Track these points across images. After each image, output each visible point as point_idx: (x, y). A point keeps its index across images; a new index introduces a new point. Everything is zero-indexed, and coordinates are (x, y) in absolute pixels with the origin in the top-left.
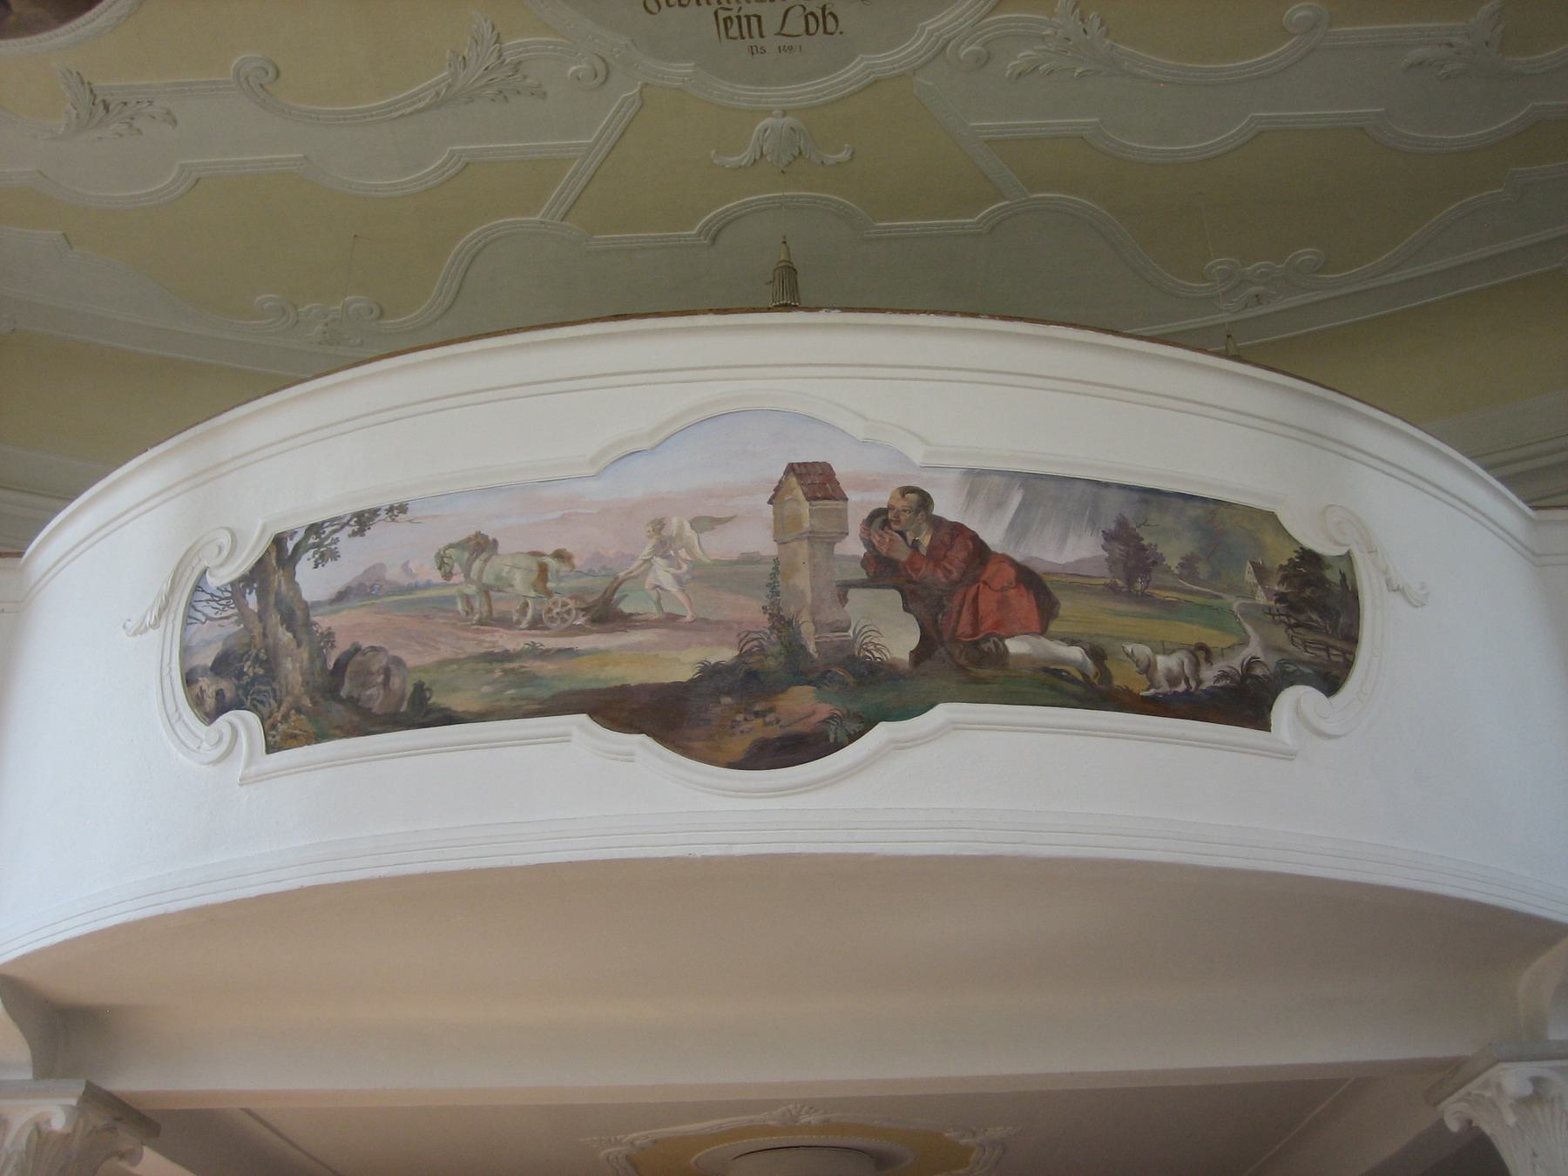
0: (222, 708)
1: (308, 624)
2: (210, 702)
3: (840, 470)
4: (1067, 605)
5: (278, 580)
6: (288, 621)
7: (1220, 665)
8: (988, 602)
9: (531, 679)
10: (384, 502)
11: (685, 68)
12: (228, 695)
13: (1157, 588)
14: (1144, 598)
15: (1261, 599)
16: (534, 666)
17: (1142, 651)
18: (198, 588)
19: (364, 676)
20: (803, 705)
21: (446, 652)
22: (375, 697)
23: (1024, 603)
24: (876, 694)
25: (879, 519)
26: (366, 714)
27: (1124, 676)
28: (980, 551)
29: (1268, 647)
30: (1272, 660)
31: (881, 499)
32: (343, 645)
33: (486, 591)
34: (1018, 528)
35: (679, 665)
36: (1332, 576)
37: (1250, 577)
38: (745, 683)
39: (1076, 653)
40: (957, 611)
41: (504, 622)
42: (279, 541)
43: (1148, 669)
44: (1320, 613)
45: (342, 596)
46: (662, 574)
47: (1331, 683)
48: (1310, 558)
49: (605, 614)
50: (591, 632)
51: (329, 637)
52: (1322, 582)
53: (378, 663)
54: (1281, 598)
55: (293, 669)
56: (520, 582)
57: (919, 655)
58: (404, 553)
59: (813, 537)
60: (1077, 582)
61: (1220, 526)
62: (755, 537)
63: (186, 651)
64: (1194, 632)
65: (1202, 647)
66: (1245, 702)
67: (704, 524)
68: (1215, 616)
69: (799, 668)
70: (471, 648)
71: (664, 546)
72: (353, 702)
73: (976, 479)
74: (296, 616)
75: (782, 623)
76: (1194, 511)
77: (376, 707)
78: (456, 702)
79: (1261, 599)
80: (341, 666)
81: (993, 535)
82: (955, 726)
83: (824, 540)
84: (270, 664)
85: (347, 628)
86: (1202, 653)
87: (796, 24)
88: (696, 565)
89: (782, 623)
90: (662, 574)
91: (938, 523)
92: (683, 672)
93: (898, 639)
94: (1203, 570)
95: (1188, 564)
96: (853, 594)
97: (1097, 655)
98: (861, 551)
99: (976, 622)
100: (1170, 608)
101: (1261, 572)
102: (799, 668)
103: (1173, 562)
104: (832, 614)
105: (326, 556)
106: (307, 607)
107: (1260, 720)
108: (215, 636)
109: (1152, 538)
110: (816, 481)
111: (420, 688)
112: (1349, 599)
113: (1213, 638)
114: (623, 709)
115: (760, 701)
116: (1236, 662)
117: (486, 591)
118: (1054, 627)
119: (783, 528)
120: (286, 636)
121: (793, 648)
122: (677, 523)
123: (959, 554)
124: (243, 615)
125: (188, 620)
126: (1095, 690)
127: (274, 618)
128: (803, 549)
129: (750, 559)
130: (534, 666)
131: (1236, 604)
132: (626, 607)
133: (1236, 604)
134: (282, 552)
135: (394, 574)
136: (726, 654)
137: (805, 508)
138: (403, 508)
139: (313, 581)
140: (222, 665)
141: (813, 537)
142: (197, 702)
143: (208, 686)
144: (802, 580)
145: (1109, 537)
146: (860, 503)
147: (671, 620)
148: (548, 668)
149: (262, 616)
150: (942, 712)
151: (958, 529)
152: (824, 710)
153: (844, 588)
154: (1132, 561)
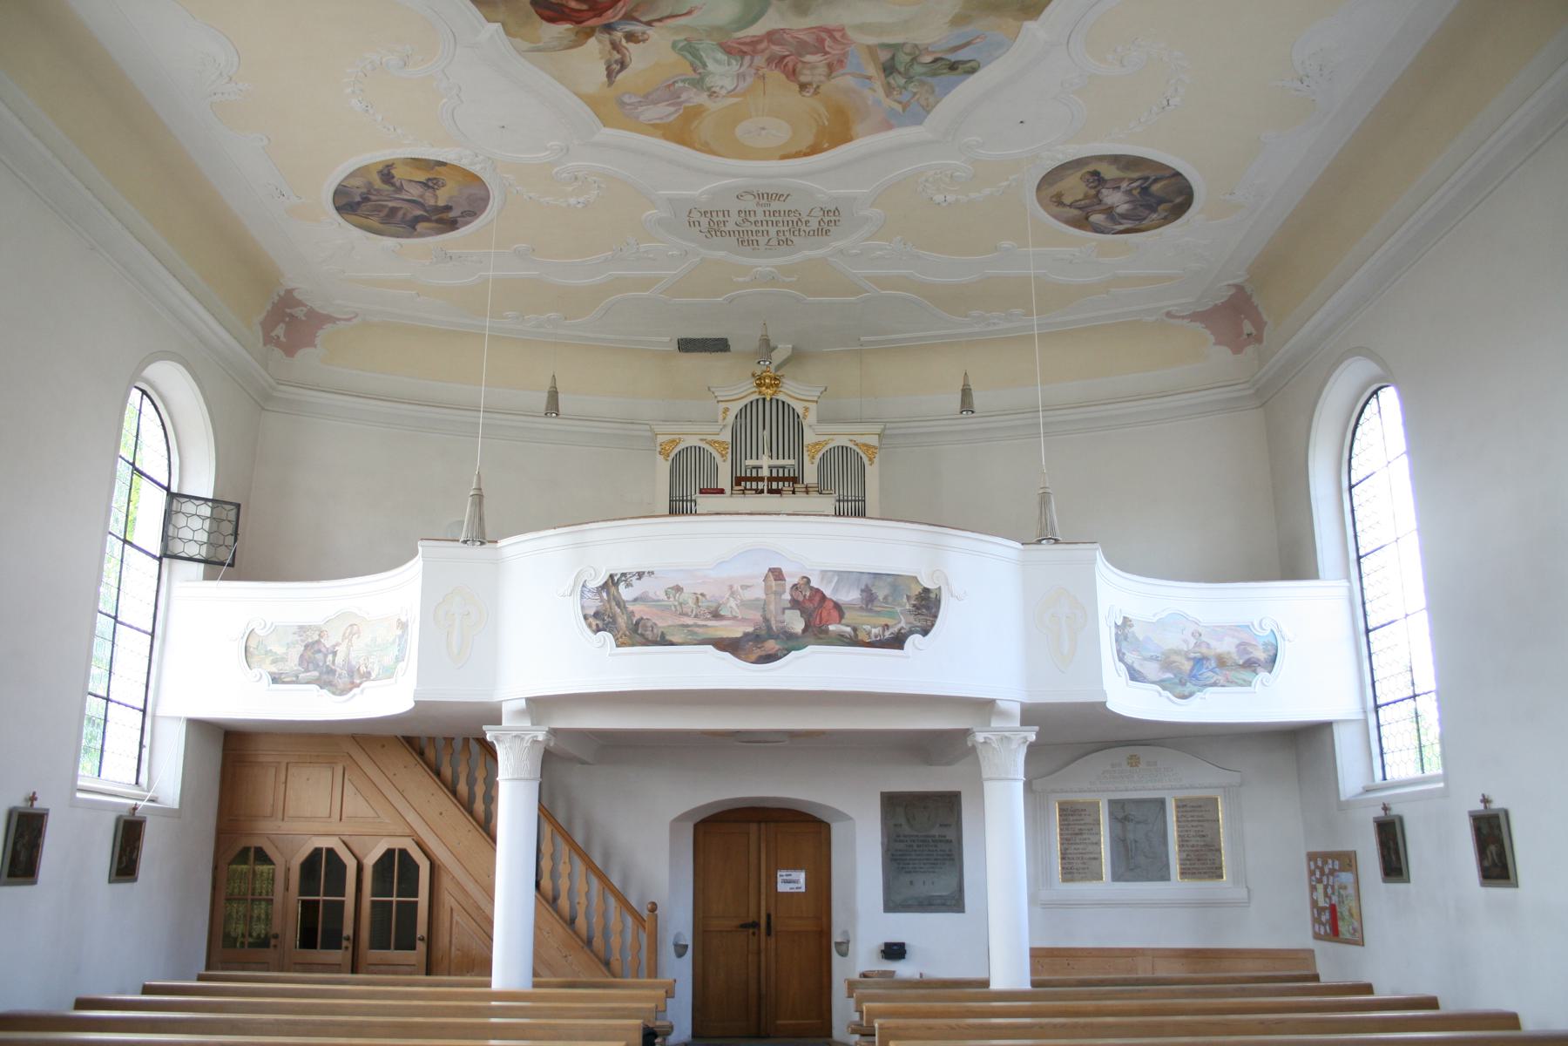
0: (598, 630)
4: (847, 615)
5: (613, 590)
6: (618, 604)
8: (825, 614)
11: (722, 253)
14: (871, 610)
19: (645, 627)
20: (772, 645)
22: (649, 634)
23: (835, 614)
24: (791, 642)
25: (795, 587)
27: (862, 636)
28: (823, 597)
30: (907, 627)
31: (796, 581)
32: (637, 617)
34: (836, 590)
35: (737, 632)
36: (933, 596)
38: (756, 638)
40: (816, 616)
41: (686, 615)
43: (869, 633)
44: (927, 606)
45: (635, 600)
47: (925, 632)
48: (926, 590)
49: (716, 615)
55: (622, 621)
56: (691, 603)
57: (804, 631)
58: (654, 588)
59: (776, 593)
60: (851, 607)
61: (896, 582)
62: (758, 593)
66: (897, 642)
67: (744, 587)
68: (892, 615)
69: (771, 635)
71: (733, 594)
74: (620, 603)
75: (766, 620)
76: (890, 579)
78: (674, 639)
80: (637, 623)
81: (828, 593)
83: (779, 594)
84: (614, 622)
85: (639, 610)
86: (887, 626)
87: (774, 242)
89: (766, 620)
90: (732, 603)
92: (739, 635)
93: (797, 624)
95: (886, 598)
97: (855, 630)
101: (908, 598)
102: (771, 635)
104: (780, 618)
105: (628, 585)
107: (901, 647)
108: (594, 605)
109: (874, 589)
110: (777, 574)
112: (938, 602)
113: (890, 622)
115: (758, 645)
119: (767, 589)
121: (769, 628)
122: (737, 587)
123: (817, 598)
124: (602, 600)
126: (854, 641)
131: (898, 609)
133: (898, 609)
134: (612, 582)
135: (651, 595)
136: (750, 629)
139: (625, 593)
140: (596, 615)
141: (776, 593)
142: (590, 626)
143: (594, 622)
144: (772, 607)
146: (790, 581)
147: (735, 618)
148: (700, 630)
150: (810, 648)
151: (818, 591)
154: (869, 597)
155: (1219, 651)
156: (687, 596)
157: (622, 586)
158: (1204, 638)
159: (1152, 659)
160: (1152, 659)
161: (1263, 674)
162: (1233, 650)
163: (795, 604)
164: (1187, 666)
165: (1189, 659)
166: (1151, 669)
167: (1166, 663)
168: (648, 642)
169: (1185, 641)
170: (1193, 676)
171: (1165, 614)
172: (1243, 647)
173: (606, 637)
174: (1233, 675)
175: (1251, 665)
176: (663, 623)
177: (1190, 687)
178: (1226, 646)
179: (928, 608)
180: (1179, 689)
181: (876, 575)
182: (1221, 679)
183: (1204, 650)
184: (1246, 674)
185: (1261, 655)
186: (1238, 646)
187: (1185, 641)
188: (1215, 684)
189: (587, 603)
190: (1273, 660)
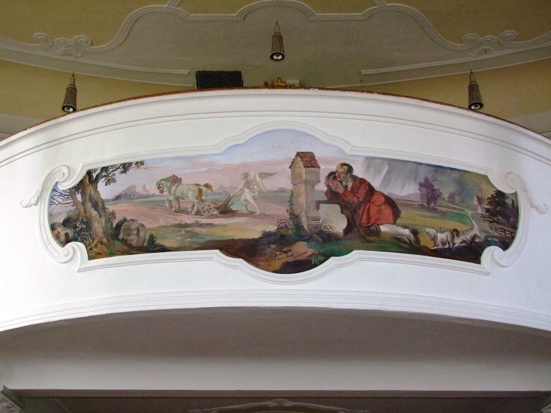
0: (68, 240)
1: (104, 208)
2: (63, 238)
3: (317, 155)
4: (404, 213)
5: (90, 189)
6: (95, 206)
7: (462, 238)
8: (373, 211)
9: (197, 235)
10: (134, 160)
12: (71, 235)
13: (439, 206)
14: (434, 210)
15: (480, 211)
16: (198, 230)
17: (432, 231)
18: (54, 190)
19: (129, 231)
20: (302, 249)
21: (162, 223)
22: (134, 240)
23: (387, 211)
24: (329, 246)
25: (332, 175)
26: (130, 246)
27: (425, 241)
28: (371, 190)
29: (481, 231)
30: (482, 236)
31: (333, 168)
32: (119, 218)
33: (177, 199)
34: (386, 181)
35: (254, 232)
36: (509, 201)
37: (476, 202)
39: (407, 232)
40: (362, 214)
41: (185, 212)
42: (89, 173)
43: (434, 239)
44: (504, 215)
46: (248, 195)
47: (505, 245)
48: (500, 195)
49: (225, 211)
50: (220, 217)
51: (113, 214)
52: (504, 204)
53: (134, 226)
54: (488, 211)
55: (99, 226)
56: (192, 196)
57: (347, 231)
58: (142, 182)
59: (306, 182)
60: (408, 204)
61: (465, 181)
63: (50, 216)
64: (452, 224)
65: (455, 230)
66: (471, 253)
67: (264, 175)
68: (461, 218)
70: (172, 222)
71: (248, 184)
72: (124, 241)
73: (370, 161)
74: (98, 205)
75: (294, 216)
76: (455, 175)
77: (134, 244)
78: (167, 243)
79: (480, 211)
80: (119, 226)
81: (376, 184)
82: (361, 259)
83: (311, 184)
84: (88, 224)
85: (121, 211)
86: (455, 232)
88: (261, 192)
89: (294, 216)
90: (248, 195)
91: (355, 178)
92: (256, 235)
93: (338, 223)
94: (457, 199)
95: (452, 196)
96: (322, 206)
97: (415, 232)
98: (325, 189)
99: (369, 219)
100: (444, 214)
101: (480, 200)
102: (301, 235)
103: (446, 196)
104: (313, 213)
106: (103, 201)
107: (477, 260)
108: (64, 210)
109: (437, 185)
110: (308, 160)
111: (152, 237)
112: (515, 211)
113: (460, 227)
114: (234, 248)
115: (284, 248)
116: (468, 237)
117: (177, 199)
118: (399, 221)
119: (295, 178)
120: (94, 213)
121: (299, 227)
123: (362, 191)
124: (75, 203)
125: (51, 203)
126: (414, 247)
127: (89, 205)
128: (302, 188)
129: (283, 191)
130: (198, 230)
131: (469, 213)
132: (233, 208)
133: (469, 213)
134: (90, 179)
135: (139, 190)
136: (272, 228)
137: (303, 170)
138: (142, 163)
139: (105, 191)
140: (67, 223)
141: (306, 182)
142: (57, 237)
144: (302, 200)
145: (421, 185)
146: (325, 169)
147: (251, 214)
148: (203, 231)
149: (83, 204)
150: (355, 254)
151: (363, 181)
152: (310, 251)
153: (319, 203)
154: (430, 193)
156: (187, 189)
157: (101, 185)
163: (333, 197)
168: (131, 249)
173: (78, 248)
176: (151, 223)
179: (505, 216)
181: (438, 168)
189: (57, 209)
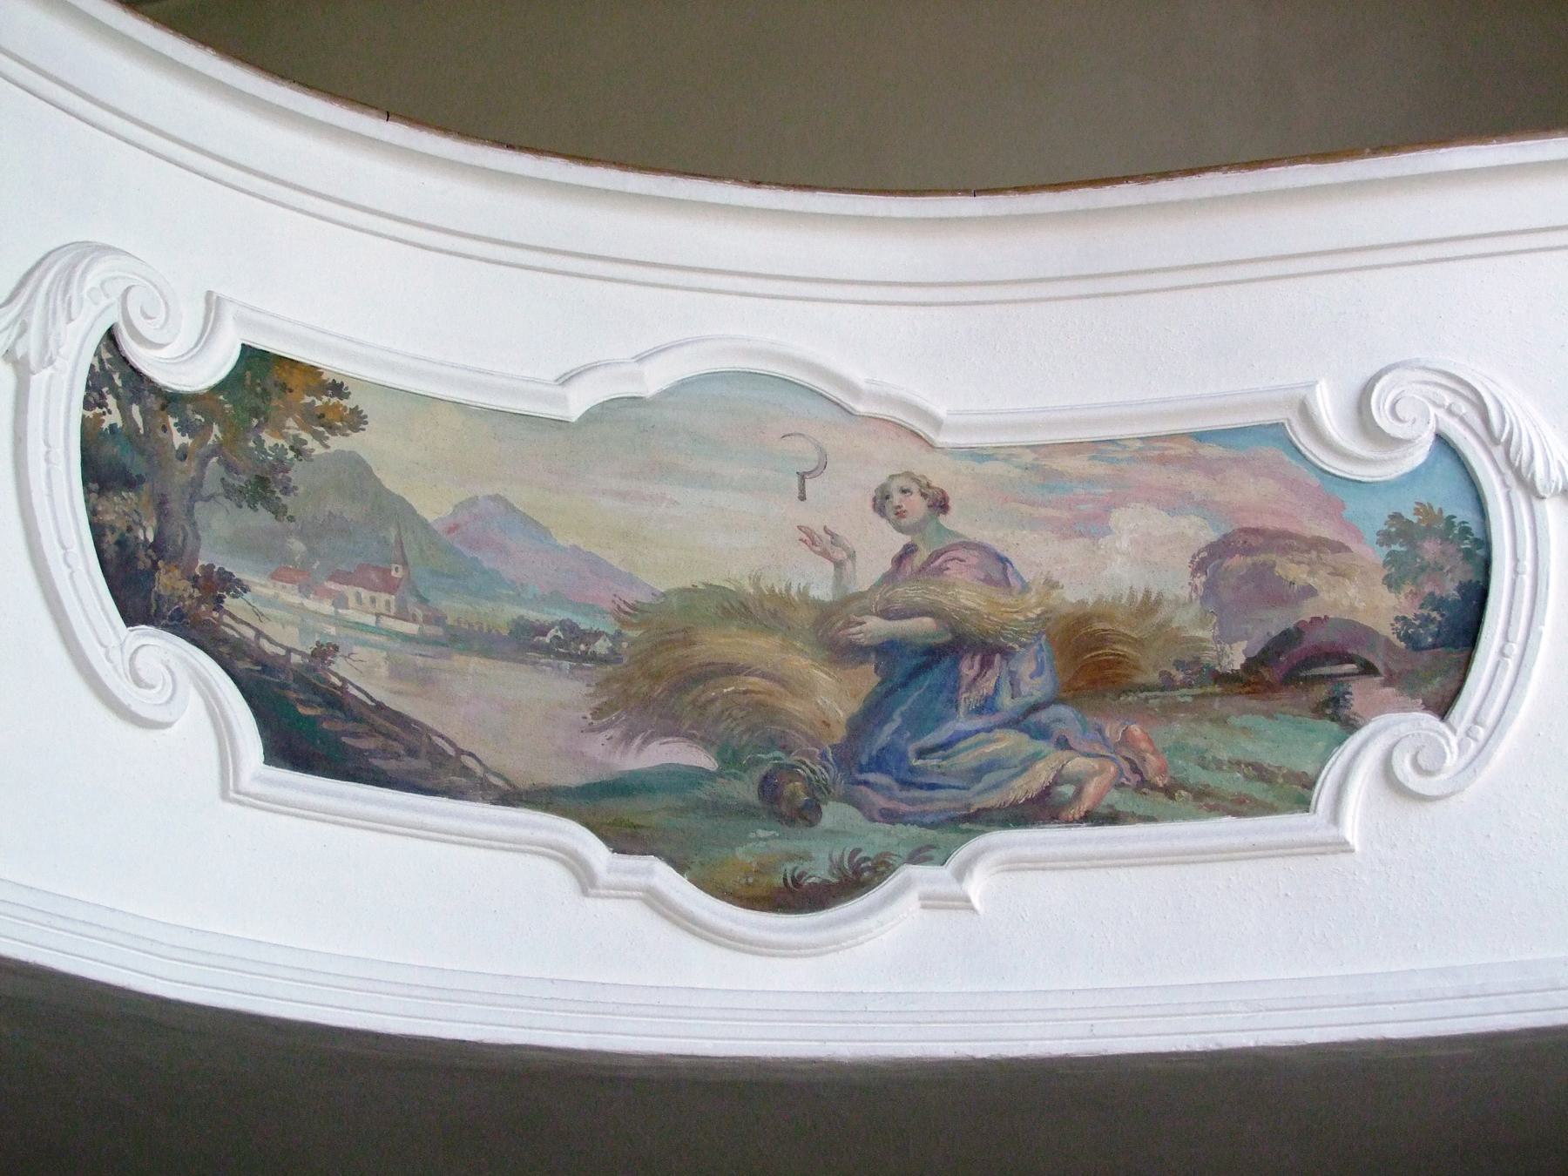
155: (1075, 594)
158: (955, 521)
159: (525, 642)
160: (525, 642)
161: (1392, 731)
162: (1176, 582)
164: (831, 697)
165: (844, 653)
166: (478, 704)
167: (660, 663)
169: (823, 543)
170: (863, 757)
171: (654, 380)
172: (1241, 560)
174: (1162, 740)
175: (1309, 675)
177: (843, 829)
178: (1133, 561)
180: (763, 845)
182: (1093, 773)
183: (966, 594)
184: (1266, 734)
185: (1371, 602)
186: (1209, 559)
187: (823, 543)
188: (1041, 809)
190: (1462, 624)
